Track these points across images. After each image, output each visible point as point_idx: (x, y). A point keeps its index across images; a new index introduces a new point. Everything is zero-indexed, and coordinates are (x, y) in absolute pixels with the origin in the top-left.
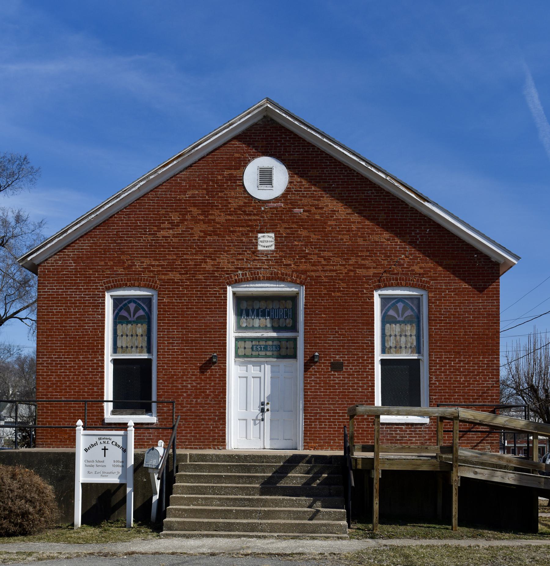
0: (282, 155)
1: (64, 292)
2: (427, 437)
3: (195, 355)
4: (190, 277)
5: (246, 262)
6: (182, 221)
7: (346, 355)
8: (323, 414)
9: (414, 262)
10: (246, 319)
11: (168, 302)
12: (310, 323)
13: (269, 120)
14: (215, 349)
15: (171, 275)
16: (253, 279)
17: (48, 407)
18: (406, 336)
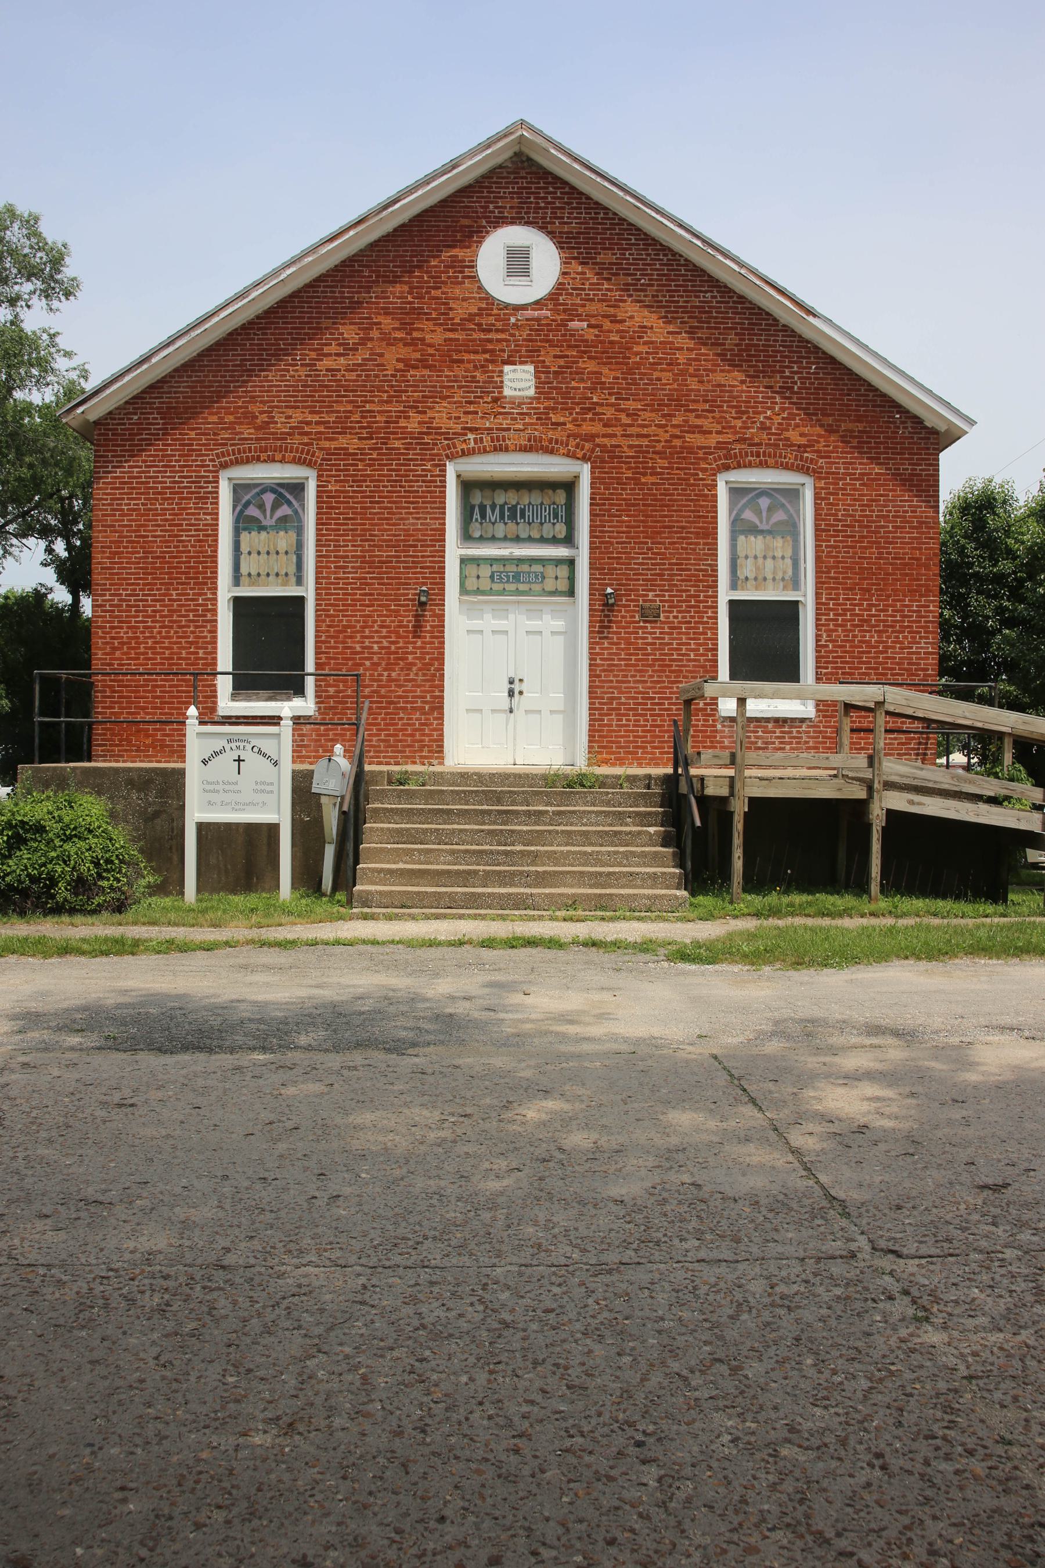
0: (549, 223)
1: (143, 472)
2: (811, 744)
3: (387, 589)
4: (377, 443)
5: (482, 418)
6: (363, 342)
7: (667, 591)
8: (623, 700)
9: (790, 425)
10: (481, 524)
11: (336, 491)
12: (600, 532)
13: (524, 159)
14: (423, 578)
15: (343, 441)
16: (495, 450)
17: (114, 686)
18: (774, 558)
